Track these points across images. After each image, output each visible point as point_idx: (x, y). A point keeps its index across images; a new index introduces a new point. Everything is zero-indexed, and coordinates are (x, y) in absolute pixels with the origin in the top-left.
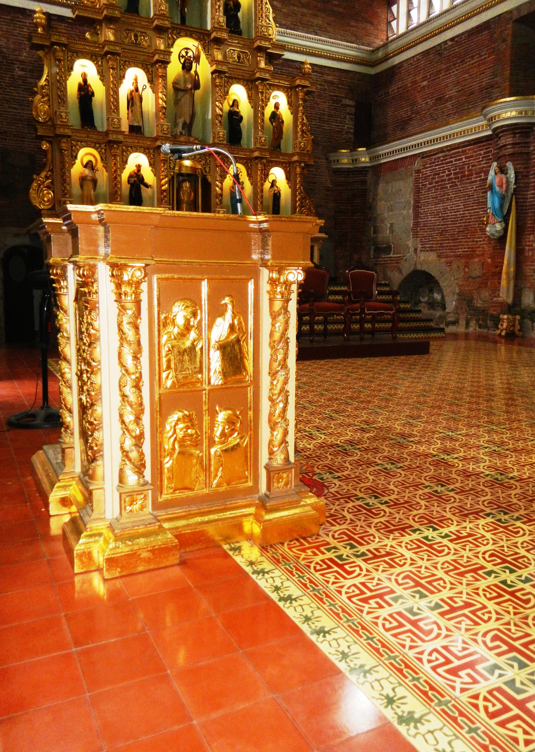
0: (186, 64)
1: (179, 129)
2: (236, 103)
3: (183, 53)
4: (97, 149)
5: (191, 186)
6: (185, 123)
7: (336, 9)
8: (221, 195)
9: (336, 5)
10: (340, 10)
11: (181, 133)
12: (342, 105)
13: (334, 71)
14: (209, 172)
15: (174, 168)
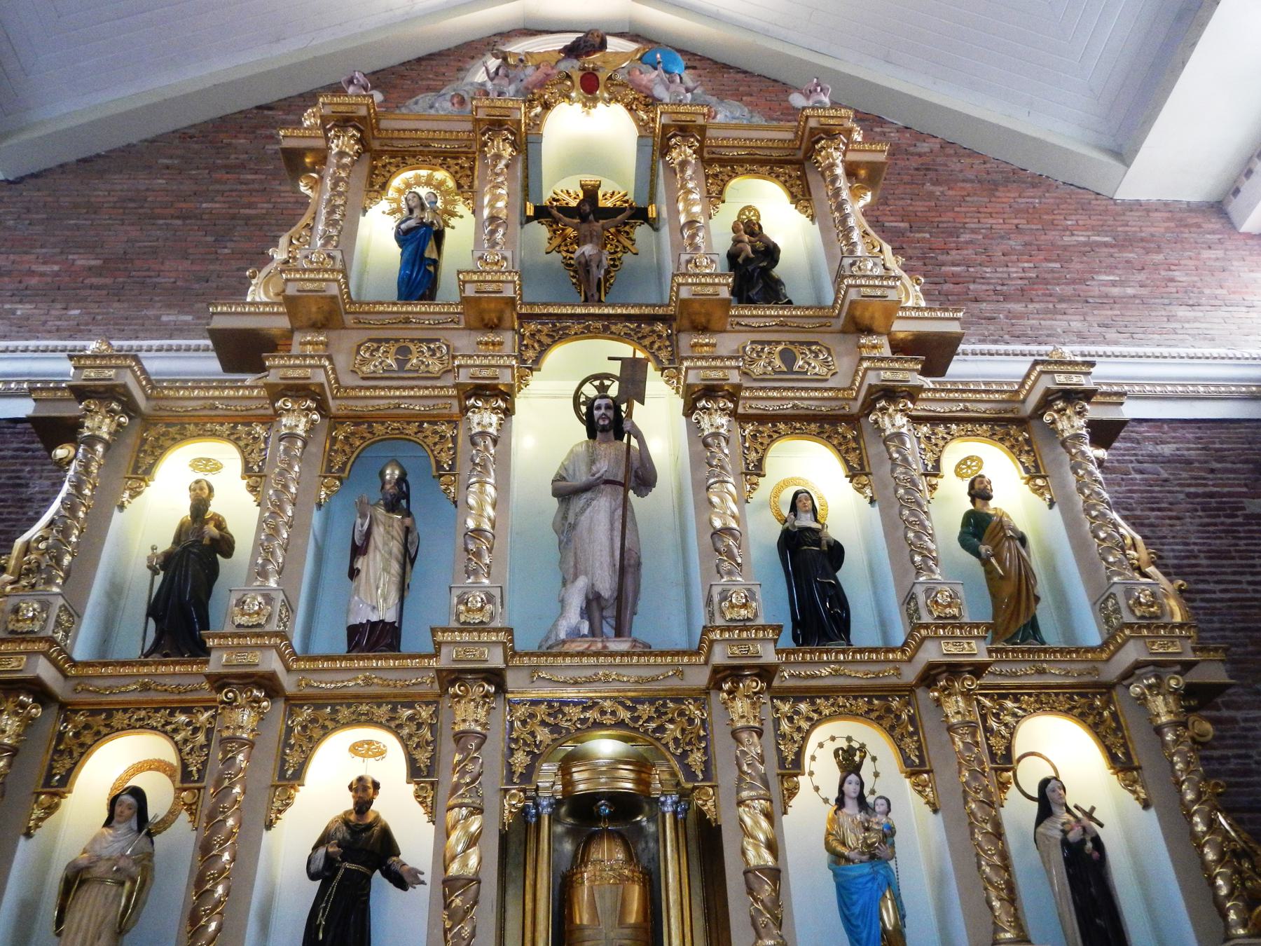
0: (597, 413)
1: (573, 617)
2: (803, 503)
3: (590, 391)
4: (168, 731)
5: (631, 857)
6: (593, 603)
7: (1115, 291)
8: (775, 874)
9: (1113, 284)
10: (1130, 291)
11: (575, 634)
12: (1246, 516)
13: (1175, 430)
14: (708, 773)
15: (529, 773)
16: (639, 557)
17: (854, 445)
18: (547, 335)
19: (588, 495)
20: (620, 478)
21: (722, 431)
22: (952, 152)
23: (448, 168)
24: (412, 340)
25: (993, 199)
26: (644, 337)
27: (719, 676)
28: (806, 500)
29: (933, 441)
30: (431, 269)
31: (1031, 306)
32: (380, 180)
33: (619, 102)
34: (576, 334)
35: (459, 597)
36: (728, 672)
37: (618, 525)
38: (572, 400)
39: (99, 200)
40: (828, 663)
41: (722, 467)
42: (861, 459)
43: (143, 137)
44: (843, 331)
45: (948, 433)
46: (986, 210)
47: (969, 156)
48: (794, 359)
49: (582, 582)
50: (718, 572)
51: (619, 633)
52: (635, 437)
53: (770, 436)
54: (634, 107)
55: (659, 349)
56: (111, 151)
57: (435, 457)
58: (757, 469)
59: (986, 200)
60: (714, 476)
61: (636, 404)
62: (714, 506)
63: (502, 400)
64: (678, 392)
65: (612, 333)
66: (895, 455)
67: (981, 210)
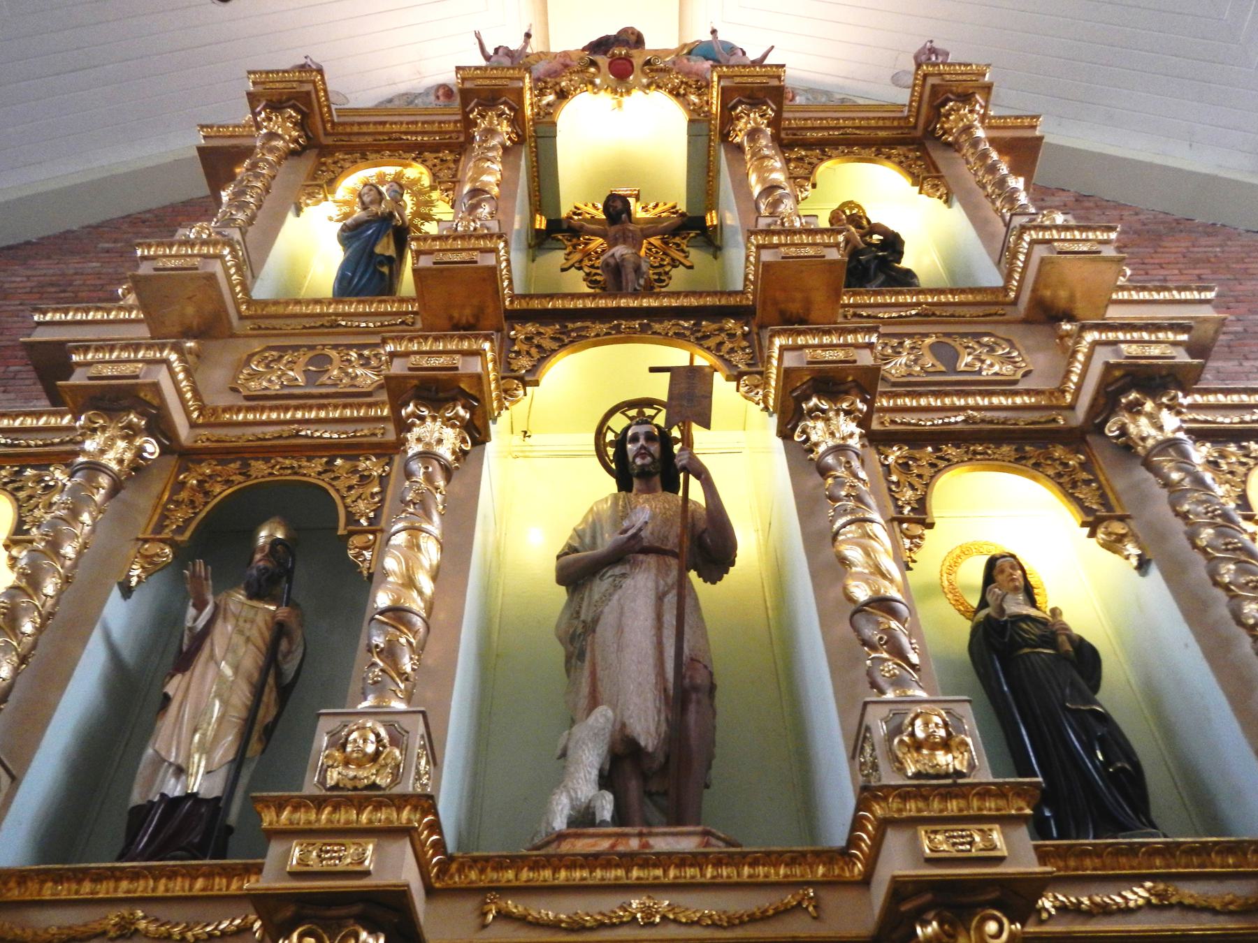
11: (583, 819)
16: (711, 674)
17: (1085, 476)
18: (551, 338)
19: (618, 570)
20: (672, 543)
21: (850, 442)
22: (1091, 204)
23: (424, 162)
24: (335, 347)
25: (1160, 250)
26: (706, 337)
28: (1012, 567)
29: (1225, 467)
30: (385, 270)
31: (1246, 364)
32: (328, 176)
33: (661, 88)
34: (598, 335)
35: (333, 734)
36: (928, 897)
37: (670, 618)
38: (594, 435)
39: (14, 285)
40: (1139, 879)
41: (859, 499)
42: (1103, 496)
43: (86, 223)
44: (1026, 321)
45: (1247, 456)
46: (1151, 261)
47: (1115, 208)
48: (956, 356)
49: (602, 716)
50: (874, 685)
51: (678, 816)
52: (698, 477)
53: (933, 465)
54: (682, 91)
55: (732, 350)
56: (43, 238)
57: (346, 507)
58: (921, 516)
59: (1151, 250)
60: (845, 512)
61: (697, 431)
62: (851, 564)
63: (464, 407)
65: (654, 333)
66: (1175, 476)
67: (1146, 261)
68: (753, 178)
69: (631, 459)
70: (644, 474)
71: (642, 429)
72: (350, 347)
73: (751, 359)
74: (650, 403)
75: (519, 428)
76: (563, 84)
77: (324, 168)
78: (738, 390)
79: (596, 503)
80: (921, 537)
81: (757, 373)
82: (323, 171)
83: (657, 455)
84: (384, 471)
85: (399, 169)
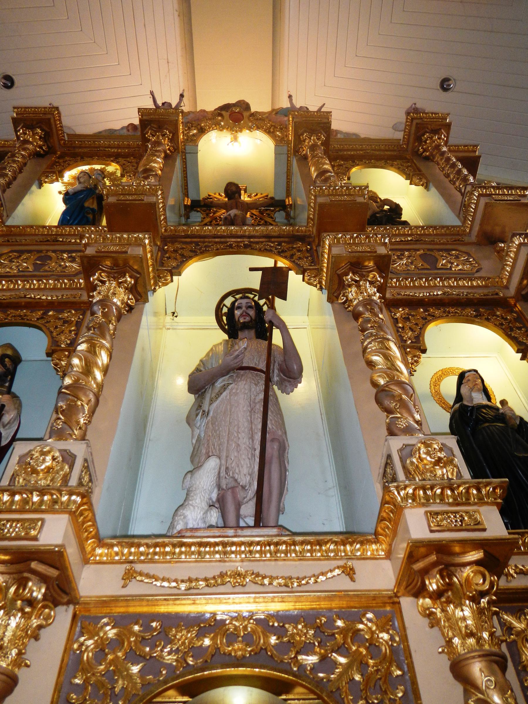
0: (237, 313)
21: (374, 298)
23: (117, 163)
24: (54, 251)
26: (283, 251)
27: (419, 566)
34: (218, 249)
36: (433, 558)
44: (478, 244)
48: (437, 260)
49: (212, 464)
55: (300, 258)
61: (278, 302)
63: (131, 277)
64: (321, 289)
68: (313, 169)
69: (237, 319)
70: (245, 326)
71: (244, 301)
72: (64, 252)
73: (312, 263)
74: (251, 290)
75: (169, 311)
76: (203, 125)
77: (57, 164)
78: (303, 280)
79: (215, 346)
80: (419, 357)
81: (315, 269)
82: (57, 166)
83: (253, 317)
84: (79, 318)
85: (103, 166)
